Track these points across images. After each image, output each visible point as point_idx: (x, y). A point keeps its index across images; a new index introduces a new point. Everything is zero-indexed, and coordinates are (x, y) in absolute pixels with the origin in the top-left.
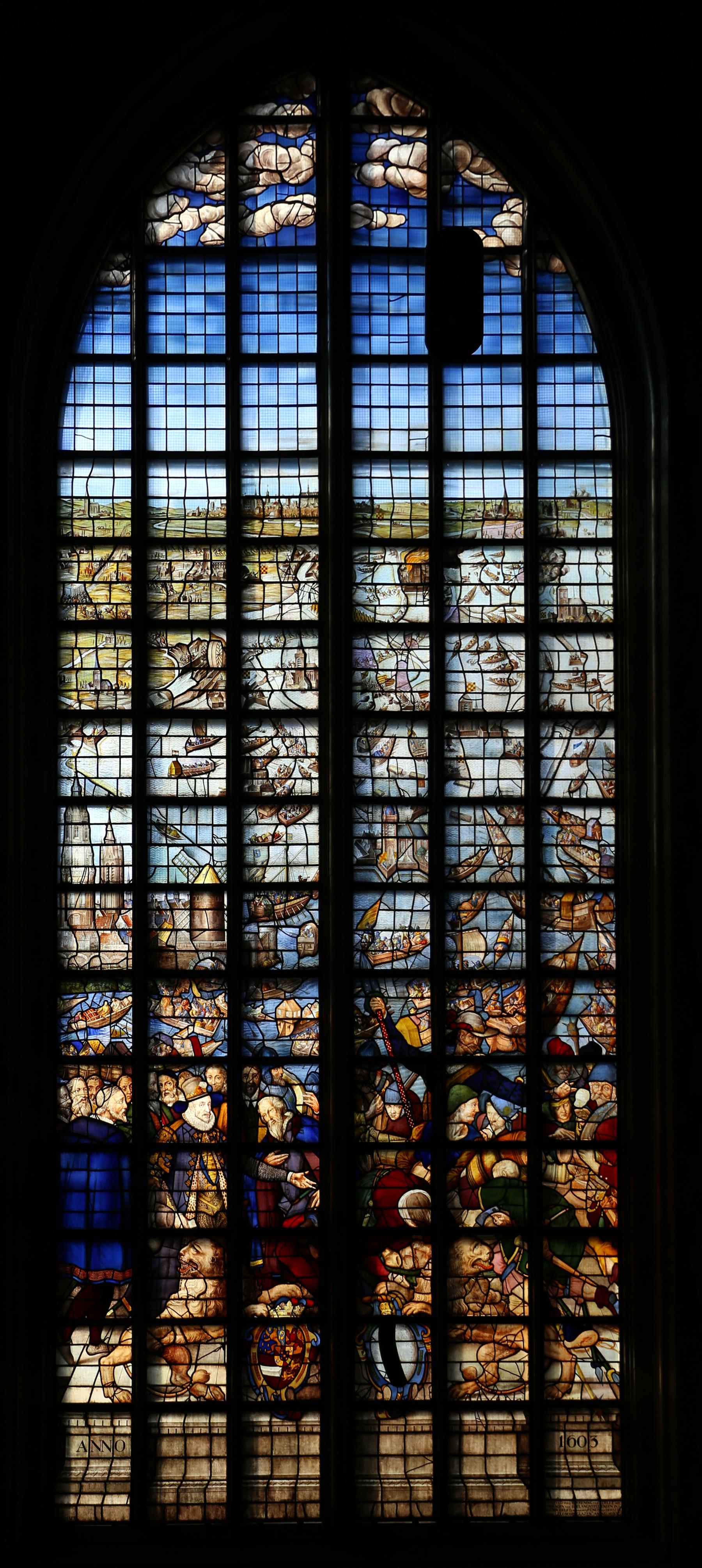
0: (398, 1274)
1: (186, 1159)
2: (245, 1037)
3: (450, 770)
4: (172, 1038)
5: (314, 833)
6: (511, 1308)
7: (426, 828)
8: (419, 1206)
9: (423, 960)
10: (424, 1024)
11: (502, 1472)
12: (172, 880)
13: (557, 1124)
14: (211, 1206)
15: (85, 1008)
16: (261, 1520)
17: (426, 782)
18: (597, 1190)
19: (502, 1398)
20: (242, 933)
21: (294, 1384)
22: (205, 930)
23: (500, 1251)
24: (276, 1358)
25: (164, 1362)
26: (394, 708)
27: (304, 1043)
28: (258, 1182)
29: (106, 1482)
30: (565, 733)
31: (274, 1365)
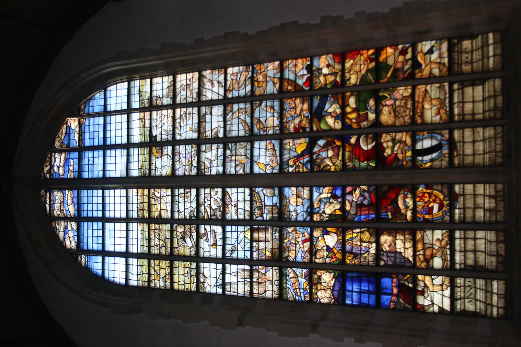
0: (394, 149)
1: (348, 247)
2: (303, 219)
3: (215, 135)
4: (303, 251)
5: (234, 190)
6: (408, 95)
7: (233, 144)
8: (367, 140)
9: (276, 143)
10: (298, 141)
11: (481, 93)
12: (249, 249)
13: (335, 81)
14: (366, 236)
15: (292, 289)
16: (504, 214)
17: (219, 145)
18: (360, 60)
19: (447, 96)
20: (267, 221)
21: (442, 197)
22: (266, 236)
23: (385, 102)
24: (430, 205)
25: (431, 260)
26: (196, 158)
27: (305, 194)
28: (357, 214)
29: (486, 291)
30: (204, 90)
31: (432, 207)
